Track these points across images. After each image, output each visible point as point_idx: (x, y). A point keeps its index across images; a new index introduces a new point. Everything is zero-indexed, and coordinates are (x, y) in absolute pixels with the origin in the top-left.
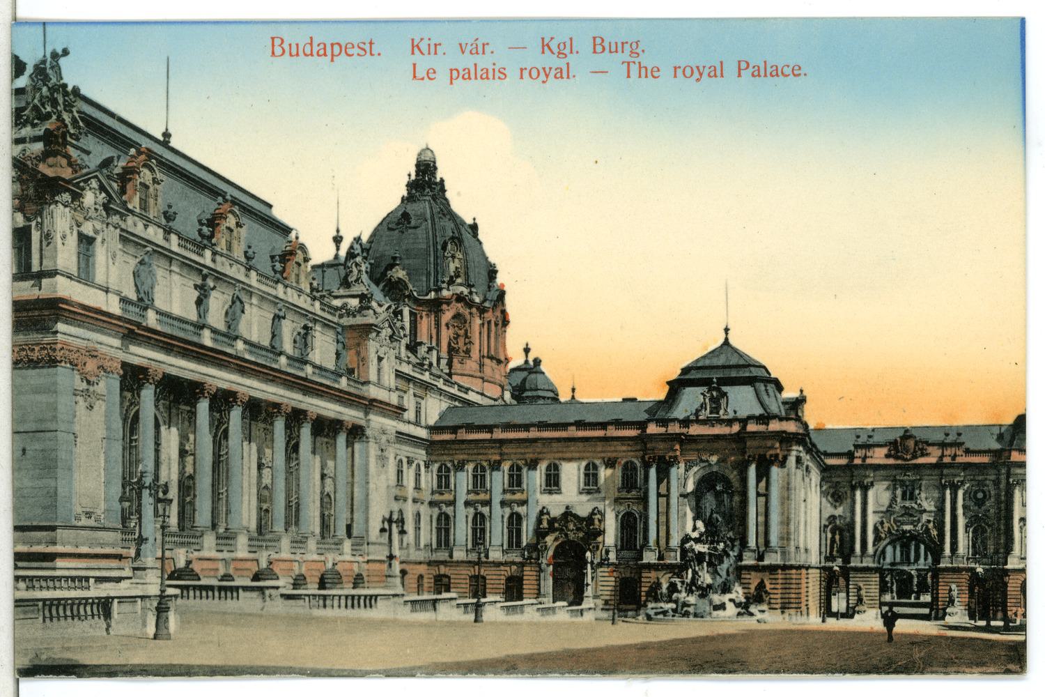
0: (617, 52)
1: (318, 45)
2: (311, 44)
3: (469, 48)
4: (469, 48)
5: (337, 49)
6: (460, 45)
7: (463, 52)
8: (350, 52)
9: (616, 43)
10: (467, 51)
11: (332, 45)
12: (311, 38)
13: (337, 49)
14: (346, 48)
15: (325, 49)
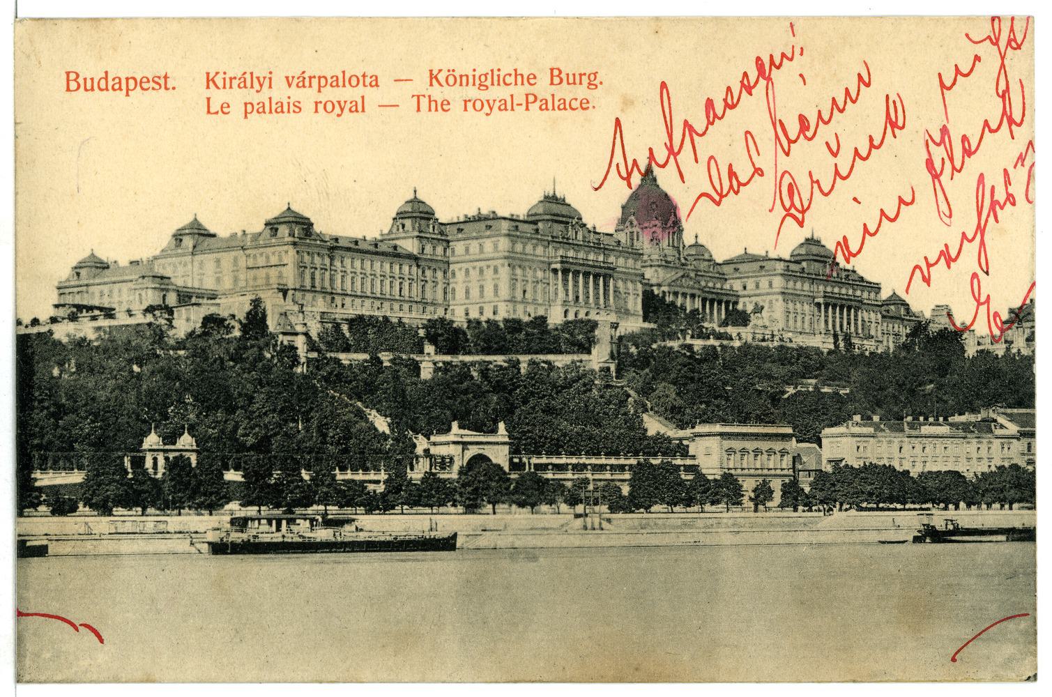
0: (574, 83)
1: (114, 79)
2: (106, 78)
3: (296, 81)
4: (296, 81)
5: (131, 82)
6: (287, 78)
7: (290, 85)
8: (145, 86)
9: (574, 75)
10: (294, 85)
11: (127, 79)
12: (106, 73)
13: (131, 82)
14: (141, 82)
15: (120, 83)
